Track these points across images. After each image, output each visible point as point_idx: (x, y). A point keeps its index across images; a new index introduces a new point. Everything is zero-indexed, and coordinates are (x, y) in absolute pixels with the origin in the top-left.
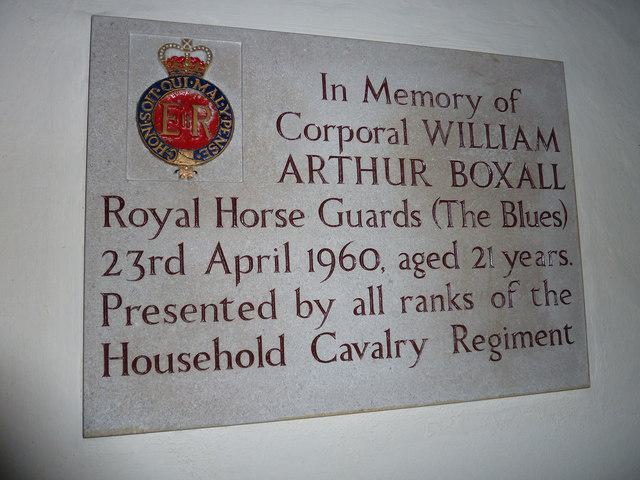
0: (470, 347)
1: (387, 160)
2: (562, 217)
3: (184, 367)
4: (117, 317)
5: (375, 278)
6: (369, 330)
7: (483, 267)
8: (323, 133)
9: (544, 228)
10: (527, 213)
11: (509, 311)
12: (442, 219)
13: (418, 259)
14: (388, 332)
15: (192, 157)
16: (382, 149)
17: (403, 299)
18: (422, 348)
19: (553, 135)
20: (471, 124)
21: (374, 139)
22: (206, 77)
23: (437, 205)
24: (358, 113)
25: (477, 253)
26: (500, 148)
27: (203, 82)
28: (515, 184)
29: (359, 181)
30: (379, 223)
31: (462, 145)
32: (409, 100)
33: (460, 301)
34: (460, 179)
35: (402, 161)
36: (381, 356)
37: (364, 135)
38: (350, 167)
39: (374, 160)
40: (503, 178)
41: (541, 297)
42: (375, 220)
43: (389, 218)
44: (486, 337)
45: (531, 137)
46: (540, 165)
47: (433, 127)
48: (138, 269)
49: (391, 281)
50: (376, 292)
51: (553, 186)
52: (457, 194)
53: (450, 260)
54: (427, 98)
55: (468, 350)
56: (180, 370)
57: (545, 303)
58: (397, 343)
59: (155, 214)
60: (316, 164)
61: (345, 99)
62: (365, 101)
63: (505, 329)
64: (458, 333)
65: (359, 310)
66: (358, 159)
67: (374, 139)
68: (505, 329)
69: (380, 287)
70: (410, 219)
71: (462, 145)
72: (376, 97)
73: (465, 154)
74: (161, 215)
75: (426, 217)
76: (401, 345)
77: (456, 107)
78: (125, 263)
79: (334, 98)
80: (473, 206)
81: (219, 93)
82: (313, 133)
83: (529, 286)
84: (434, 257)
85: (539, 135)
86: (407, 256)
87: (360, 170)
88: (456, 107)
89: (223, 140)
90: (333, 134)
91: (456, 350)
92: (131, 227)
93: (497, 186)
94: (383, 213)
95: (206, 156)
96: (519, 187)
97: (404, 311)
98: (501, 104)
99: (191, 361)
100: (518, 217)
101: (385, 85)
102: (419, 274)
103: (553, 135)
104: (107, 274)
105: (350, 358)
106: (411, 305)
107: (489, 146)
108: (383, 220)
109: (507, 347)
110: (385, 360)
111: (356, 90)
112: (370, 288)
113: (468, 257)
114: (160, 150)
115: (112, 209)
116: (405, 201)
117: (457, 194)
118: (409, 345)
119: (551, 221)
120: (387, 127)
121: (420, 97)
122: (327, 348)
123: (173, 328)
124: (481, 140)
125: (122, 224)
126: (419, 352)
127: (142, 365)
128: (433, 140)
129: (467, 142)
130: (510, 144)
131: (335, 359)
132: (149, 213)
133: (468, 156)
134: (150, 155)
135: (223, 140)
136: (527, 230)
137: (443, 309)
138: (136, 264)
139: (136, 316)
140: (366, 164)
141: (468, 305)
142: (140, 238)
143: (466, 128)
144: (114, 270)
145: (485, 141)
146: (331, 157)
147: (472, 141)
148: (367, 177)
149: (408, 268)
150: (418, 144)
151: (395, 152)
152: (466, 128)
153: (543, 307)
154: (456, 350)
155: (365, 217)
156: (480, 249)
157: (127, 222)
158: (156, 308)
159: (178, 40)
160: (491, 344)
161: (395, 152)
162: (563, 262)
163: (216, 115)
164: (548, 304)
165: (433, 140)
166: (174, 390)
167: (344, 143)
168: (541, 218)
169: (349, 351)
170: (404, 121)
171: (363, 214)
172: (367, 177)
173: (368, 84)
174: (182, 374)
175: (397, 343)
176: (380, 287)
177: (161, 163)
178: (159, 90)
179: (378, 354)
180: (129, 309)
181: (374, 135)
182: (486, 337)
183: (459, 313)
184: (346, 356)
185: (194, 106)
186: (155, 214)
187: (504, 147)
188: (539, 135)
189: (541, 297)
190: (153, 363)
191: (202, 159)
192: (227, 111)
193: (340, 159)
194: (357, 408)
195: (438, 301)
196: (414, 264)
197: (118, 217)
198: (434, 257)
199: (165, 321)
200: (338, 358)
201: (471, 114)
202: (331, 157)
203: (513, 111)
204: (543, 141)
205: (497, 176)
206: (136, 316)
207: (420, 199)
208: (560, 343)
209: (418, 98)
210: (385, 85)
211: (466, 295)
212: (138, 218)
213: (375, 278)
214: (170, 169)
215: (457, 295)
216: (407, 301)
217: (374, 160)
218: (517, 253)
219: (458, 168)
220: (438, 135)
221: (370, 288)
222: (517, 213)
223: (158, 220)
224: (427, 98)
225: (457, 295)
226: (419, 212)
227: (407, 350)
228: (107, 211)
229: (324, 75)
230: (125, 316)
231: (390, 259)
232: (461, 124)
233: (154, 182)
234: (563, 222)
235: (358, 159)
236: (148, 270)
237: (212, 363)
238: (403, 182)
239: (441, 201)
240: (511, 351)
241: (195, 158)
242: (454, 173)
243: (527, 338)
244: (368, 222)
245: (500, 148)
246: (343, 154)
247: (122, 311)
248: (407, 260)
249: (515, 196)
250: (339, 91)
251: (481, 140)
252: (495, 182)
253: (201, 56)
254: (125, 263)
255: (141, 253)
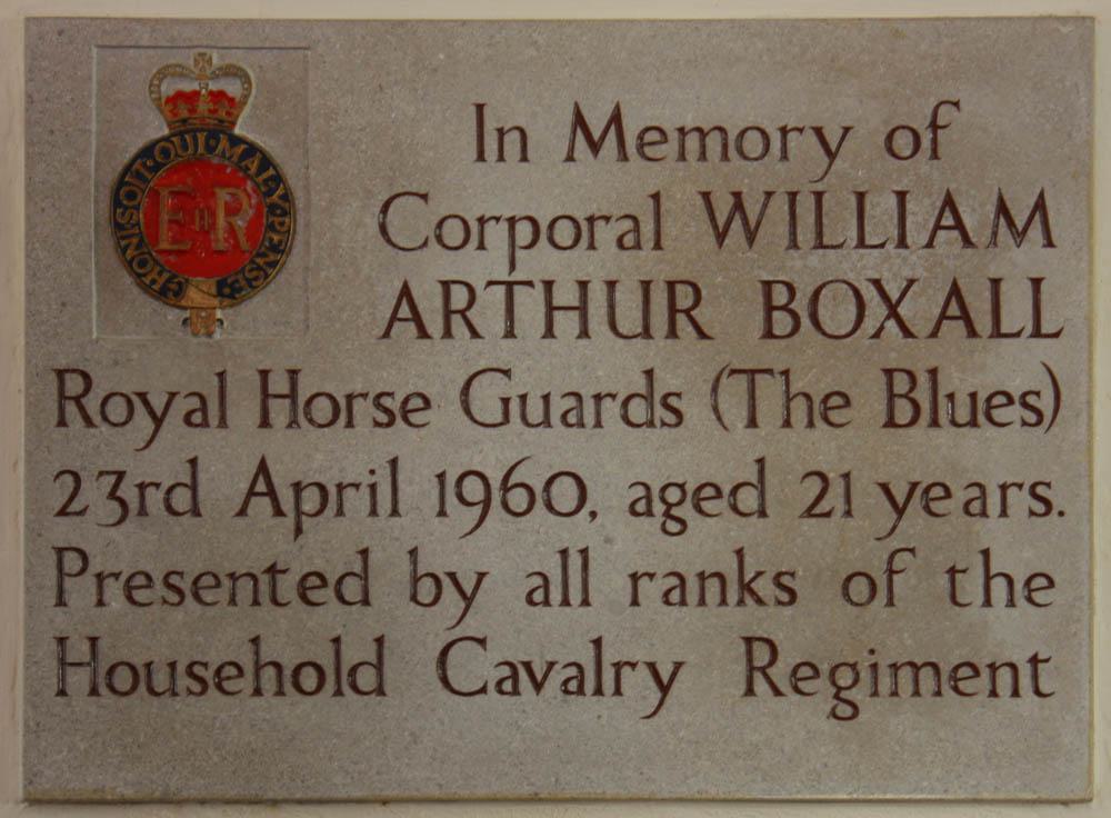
0: (784, 686)
1: (611, 285)
2: (1046, 403)
3: (196, 687)
4: (81, 591)
5: (576, 533)
6: (559, 635)
7: (828, 515)
8: (474, 233)
9: (991, 431)
10: (951, 397)
11: (885, 613)
12: (735, 411)
13: (673, 495)
14: (598, 643)
15: (214, 290)
16: (598, 264)
17: (635, 577)
18: (672, 679)
19: (1040, 206)
20: (819, 195)
21: (584, 242)
22: (237, 131)
23: (724, 380)
24: (556, 185)
25: (815, 486)
26: (890, 247)
27: (236, 141)
28: (921, 327)
29: (549, 333)
30: (589, 419)
31: (794, 245)
32: (670, 149)
33: (764, 587)
34: (782, 322)
35: (646, 286)
36: (581, 691)
37: (564, 233)
38: (530, 305)
39: (583, 285)
40: (893, 312)
41: (971, 586)
42: (580, 411)
43: (611, 409)
44: (825, 668)
45: (977, 215)
46: (996, 282)
47: (723, 207)
48: (115, 505)
49: (608, 540)
50: (575, 562)
51: (1029, 329)
52: (774, 355)
53: (748, 499)
54: (714, 142)
55: (777, 692)
56: (190, 692)
57: (980, 599)
58: (618, 666)
59: (146, 403)
60: (459, 297)
61: (524, 158)
62: (570, 158)
63: (872, 652)
64: (756, 654)
65: (538, 596)
66: (549, 285)
67: (584, 242)
68: (872, 652)
69: (584, 552)
70: (660, 412)
71: (794, 245)
72: (595, 147)
73: (798, 264)
74: (158, 404)
75: (695, 409)
76: (626, 671)
77: (784, 156)
78: (94, 493)
79: (501, 158)
80: (813, 380)
81: (266, 162)
82: (453, 233)
83: (942, 561)
84: (709, 492)
85: (1002, 209)
86: (647, 488)
87: (551, 309)
88: (784, 156)
89: (272, 257)
90: (496, 234)
91: (750, 691)
92: (104, 428)
93: (877, 335)
94: (598, 398)
95: (241, 289)
96: (934, 334)
97: (635, 602)
98: (903, 142)
99: (208, 675)
100: (926, 406)
101: (616, 119)
102: (673, 527)
103: (1040, 206)
104: (63, 512)
105: (516, 692)
106: (651, 591)
107: (861, 243)
108: (598, 414)
109: (875, 694)
110: (589, 700)
111: (551, 133)
112: (564, 553)
113: (790, 493)
114: (154, 282)
115: (69, 394)
116: (649, 373)
117: (774, 355)
118: (643, 673)
119: (1014, 413)
120: (617, 213)
121: (699, 139)
122: (472, 667)
123: (178, 615)
124: (842, 226)
125: (89, 422)
126: (665, 689)
127: (123, 679)
128: (721, 237)
129: (806, 235)
130: (917, 236)
131: (483, 690)
132: (136, 400)
133: (806, 268)
134: (136, 290)
135: (272, 257)
136: (945, 434)
137: (723, 602)
138: (112, 495)
139: (114, 590)
140: (566, 295)
141: (785, 597)
142: (116, 447)
143: (806, 205)
144: (75, 506)
145: (853, 234)
146: (490, 283)
147: (820, 234)
148: (566, 323)
149: (649, 513)
150: (688, 246)
151: (633, 267)
152: (806, 205)
153: (975, 612)
154: (750, 691)
155: (559, 406)
156: (822, 476)
157: (97, 419)
158: (148, 577)
159: (187, 59)
160: (834, 683)
161: (633, 267)
162: (1039, 508)
163: (259, 208)
164: (988, 603)
165: (721, 237)
166: (178, 726)
167: (520, 254)
168: (983, 410)
169: (515, 676)
170: (656, 197)
171: (555, 399)
172: (566, 323)
173: (579, 121)
174: (192, 699)
175: (618, 666)
176: (584, 552)
177: (156, 304)
178: (149, 163)
179: (575, 686)
180: (100, 577)
181: (585, 230)
182: (825, 668)
183: (761, 611)
184: (508, 686)
185: (217, 190)
186: (146, 403)
187: (902, 243)
188: (1002, 209)
189: (971, 586)
190: (141, 676)
191: (232, 296)
192: (281, 197)
193: (510, 285)
194: (526, 790)
195: (713, 586)
196: (665, 505)
197: (82, 409)
198: (709, 492)
199: (165, 601)
200: (491, 687)
201: (820, 172)
202: (490, 283)
203: (935, 155)
204: (1011, 223)
205: (876, 310)
206: (114, 590)
207: (682, 367)
208: (1016, 693)
209: (692, 142)
210: (616, 119)
211: (780, 574)
212: (117, 410)
213: (576, 533)
214: (174, 316)
215: (759, 574)
216: (644, 583)
217: (583, 285)
218: (914, 486)
219: (780, 296)
220: (737, 224)
221: (564, 553)
222: (923, 395)
223: (151, 412)
224: (714, 142)
225: (759, 574)
226: (678, 395)
227: (637, 680)
228: (62, 396)
229: (480, 108)
230: (94, 590)
231: (611, 494)
232: (793, 196)
233: (146, 345)
234: (1048, 414)
235: (549, 285)
236: (134, 505)
237: (246, 684)
238: (646, 333)
239: (733, 372)
240: (884, 701)
241: (220, 294)
242: (770, 308)
243: (926, 675)
244: (564, 416)
245: (890, 247)
246: (518, 276)
247: (89, 580)
248: (648, 498)
249: (920, 356)
250: (513, 139)
251: (842, 226)
252: (870, 325)
253: (233, 88)
254: (94, 493)
255: (120, 475)
